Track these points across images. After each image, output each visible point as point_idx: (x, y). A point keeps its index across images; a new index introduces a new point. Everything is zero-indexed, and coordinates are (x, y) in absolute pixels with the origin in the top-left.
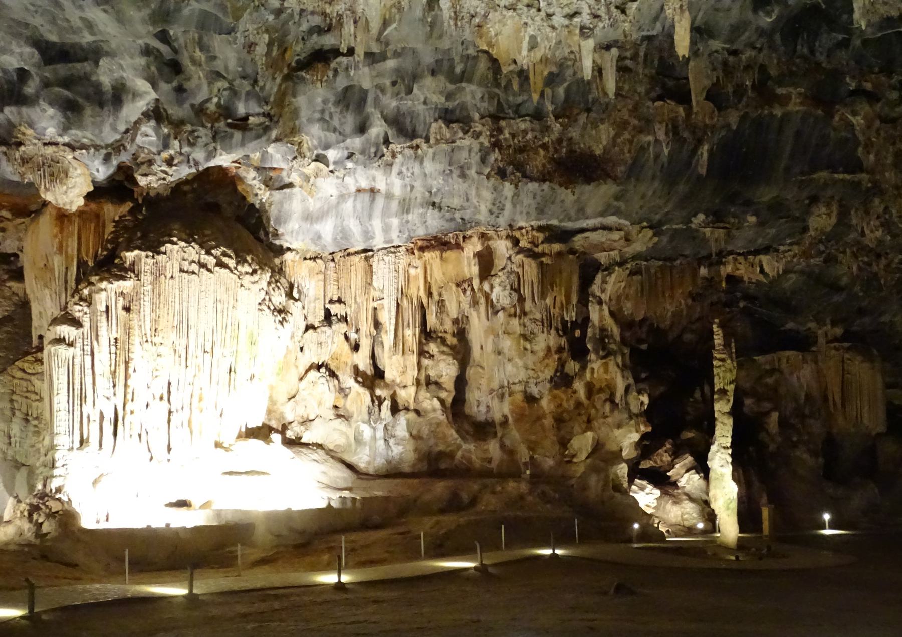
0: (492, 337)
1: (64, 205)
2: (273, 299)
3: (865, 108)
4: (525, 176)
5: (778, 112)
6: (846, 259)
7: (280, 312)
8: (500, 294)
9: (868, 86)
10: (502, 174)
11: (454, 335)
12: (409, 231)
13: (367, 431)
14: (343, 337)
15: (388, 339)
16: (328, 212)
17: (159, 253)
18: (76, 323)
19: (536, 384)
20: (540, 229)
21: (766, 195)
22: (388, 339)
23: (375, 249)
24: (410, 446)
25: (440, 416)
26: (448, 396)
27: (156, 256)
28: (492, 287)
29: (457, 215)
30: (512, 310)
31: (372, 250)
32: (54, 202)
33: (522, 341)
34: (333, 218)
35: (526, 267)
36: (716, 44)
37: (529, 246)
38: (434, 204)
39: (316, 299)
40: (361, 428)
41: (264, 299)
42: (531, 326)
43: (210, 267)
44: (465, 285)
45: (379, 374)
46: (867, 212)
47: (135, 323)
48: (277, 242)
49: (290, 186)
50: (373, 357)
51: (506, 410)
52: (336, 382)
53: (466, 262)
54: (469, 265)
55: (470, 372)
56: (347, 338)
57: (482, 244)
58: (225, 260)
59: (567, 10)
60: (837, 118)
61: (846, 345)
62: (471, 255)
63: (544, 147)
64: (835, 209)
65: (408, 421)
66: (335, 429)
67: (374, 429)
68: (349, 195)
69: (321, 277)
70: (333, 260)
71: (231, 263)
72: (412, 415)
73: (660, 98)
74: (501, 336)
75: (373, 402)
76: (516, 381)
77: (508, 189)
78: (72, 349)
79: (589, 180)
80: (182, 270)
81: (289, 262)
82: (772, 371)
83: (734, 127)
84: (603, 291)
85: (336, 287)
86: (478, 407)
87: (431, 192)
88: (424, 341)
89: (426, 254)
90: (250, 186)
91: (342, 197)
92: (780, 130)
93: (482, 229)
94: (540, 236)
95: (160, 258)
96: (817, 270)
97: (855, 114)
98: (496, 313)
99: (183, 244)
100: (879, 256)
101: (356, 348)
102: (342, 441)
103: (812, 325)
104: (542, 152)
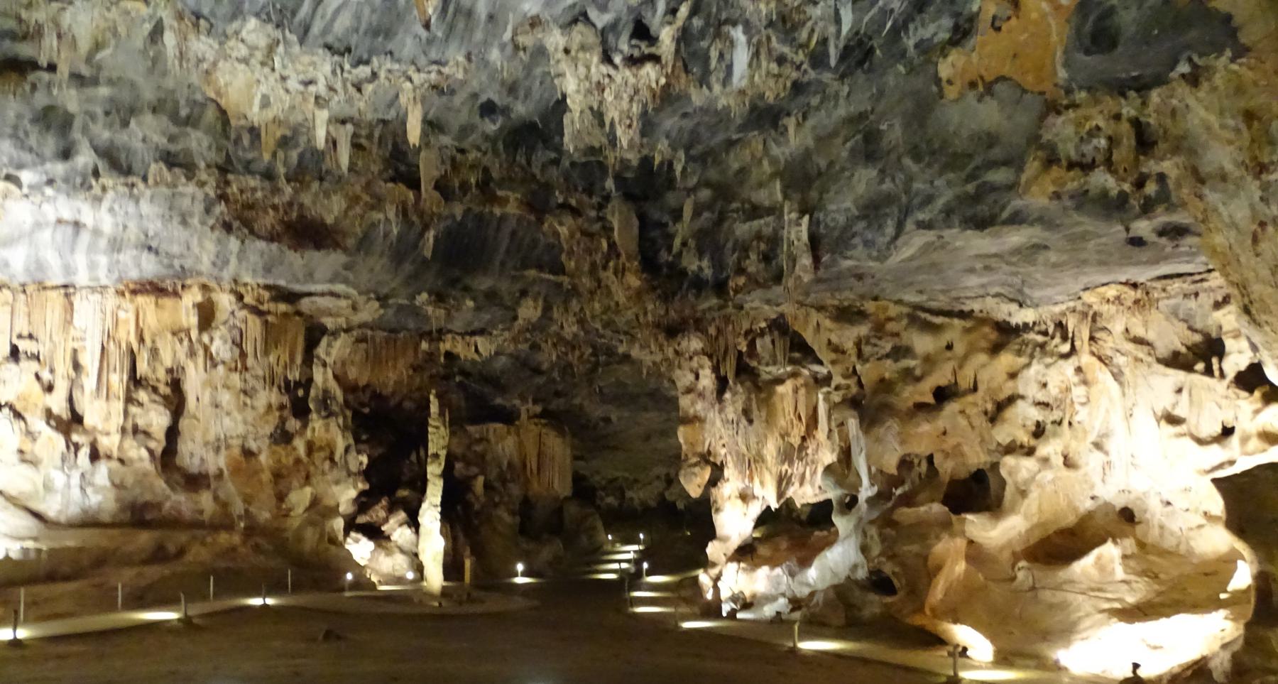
3: (569, 219)
4: (252, 232)
5: (497, 211)
6: (547, 347)
8: (220, 346)
9: (573, 202)
10: (228, 227)
11: (167, 384)
14: (33, 377)
15: (89, 381)
20: (267, 287)
21: (484, 283)
22: (89, 381)
28: (212, 340)
29: (177, 263)
30: (233, 365)
35: (250, 323)
36: (446, 140)
37: (254, 303)
38: (150, 248)
42: (252, 382)
44: (183, 335)
46: (566, 310)
53: (185, 310)
54: (188, 315)
56: (38, 377)
57: (203, 295)
59: (302, 77)
60: (546, 225)
61: (543, 421)
62: (190, 305)
63: (275, 208)
64: (540, 303)
73: (393, 180)
77: (234, 244)
79: (318, 246)
82: (481, 440)
83: (459, 218)
84: (328, 354)
92: (498, 229)
93: (204, 280)
94: (266, 295)
96: (523, 355)
97: (561, 224)
98: (215, 365)
100: (573, 348)
101: (49, 388)
103: (517, 402)
104: (271, 212)
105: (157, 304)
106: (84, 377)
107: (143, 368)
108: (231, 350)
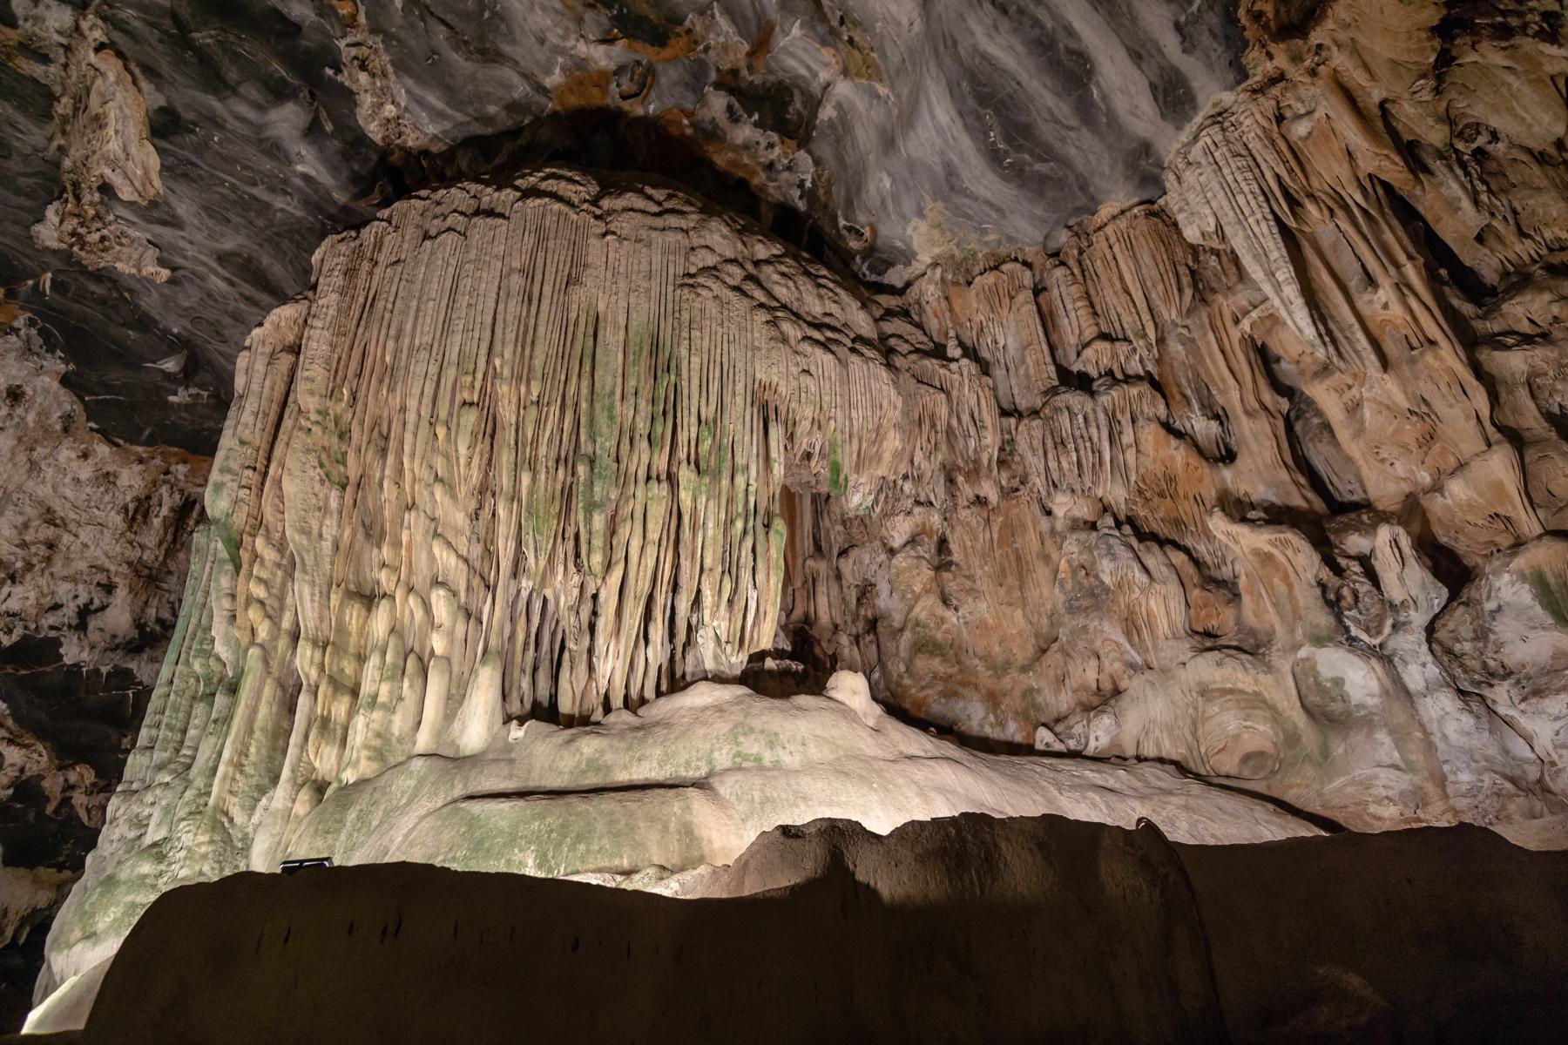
13: (1359, 680)
67: (1383, 656)
89: (1316, 37)
102: (1260, 735)
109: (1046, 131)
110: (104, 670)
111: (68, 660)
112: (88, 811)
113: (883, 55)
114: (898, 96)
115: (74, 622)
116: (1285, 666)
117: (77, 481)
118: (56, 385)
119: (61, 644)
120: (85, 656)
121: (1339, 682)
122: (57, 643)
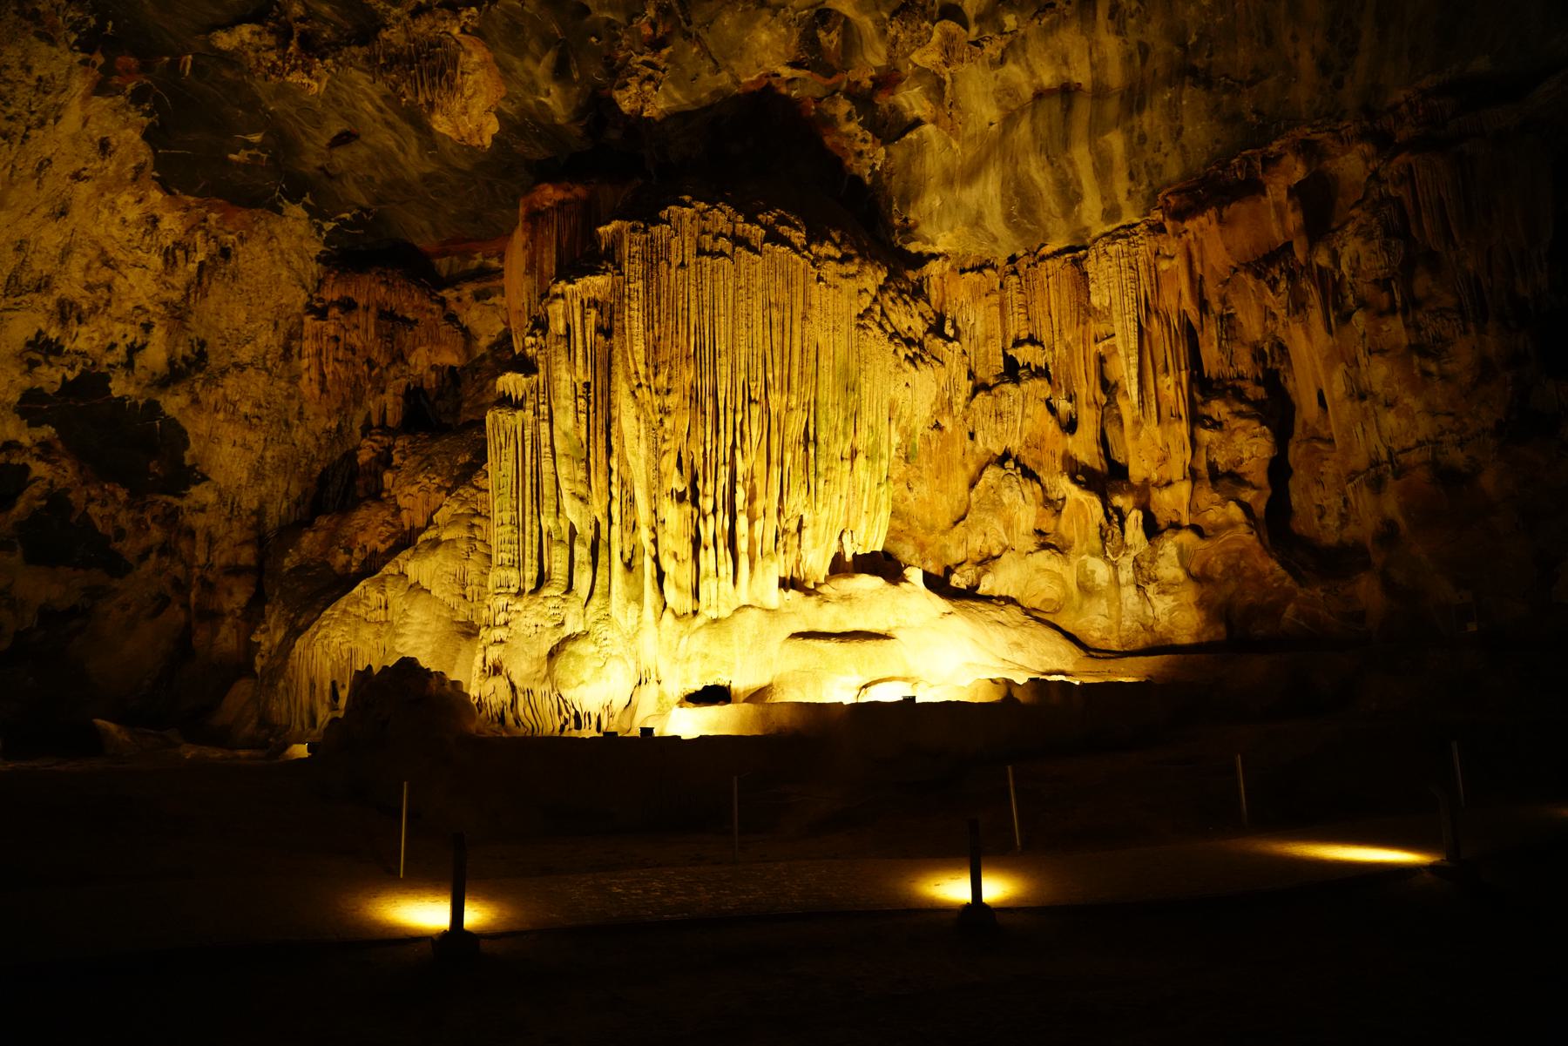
0: (1342, 366)
1: (471, 136)
2: (893, 317)
7: (909, 342)
8: (1354, 254)
11: (1257, 382)
12: (1149, 173)
13: (1101, 572)
14: (1043, 406)
16: (988, 155)
17: (657, 221)
18: (526, 366)
19: (1461, 444)
22: (1128, 407)
23: (1088, 241)
24: (1189, 594)
25: (1243, 536)
26: (1256, 497)
27: (651, 229)
28: (1335, 257)
29: (1246, 104)
30: (1384, 298)
31: (1086, 248)
32: (454, 135)
33: (1416, 360)
34: (998, 164)
38: (1193, 71)
39: (988, 338)
40: (1090, 567)
41: (869, 310)
43: (753, 243)
45: (1118, 472)
47: (617, 352)
48: (913, 247)
49: (918, 122)
50: (1103, 441)
51: (1391, 505)
52: (1037, 487)
53: (1275, 215)
54: (1281, 217)
55: (1295, 453)
56: (1052, 410)
57: (1307, 162)
58: (784, 230)
65: (1180, 548)
66: (1038, 570)
67: (1115, 566)
68: (1022, 111)
69: (995, 298)
70: (1015, 272)
71: (798, 237)
72: (1187, 537)
74: (1363, 361)
75: (1108, 518)
76: (1412, 442)
78: (519, 413)
80: (701, 252)
81: (934, 281)
85: (1023, 317)
86: (1320, 518)
87: (1183, 46)
88: (1198, 397)
89: (1188, 225)
90: (848, 135)
91: (1010, 120)
95: (655, 230)
98: (1346, 318)
99: (702, 206)
101: (1070, 426)
102: (1052, 591)
105: (1220, 220)
106: (1121, 401)
107: (1211, 354)
108: (1385, 247)
109: (1042, 215)
110: (141, 402)
111: (115, 393)
112: (102, 519)
113: (965, 128)
114: (964, 154)
115: (125, 360)
116: (1075, 562)
117: (124, 221)
118: (138, 137)
119: (110, 380)
120: (131, 391)
121: (1093, 572)
122: (106, 379)
